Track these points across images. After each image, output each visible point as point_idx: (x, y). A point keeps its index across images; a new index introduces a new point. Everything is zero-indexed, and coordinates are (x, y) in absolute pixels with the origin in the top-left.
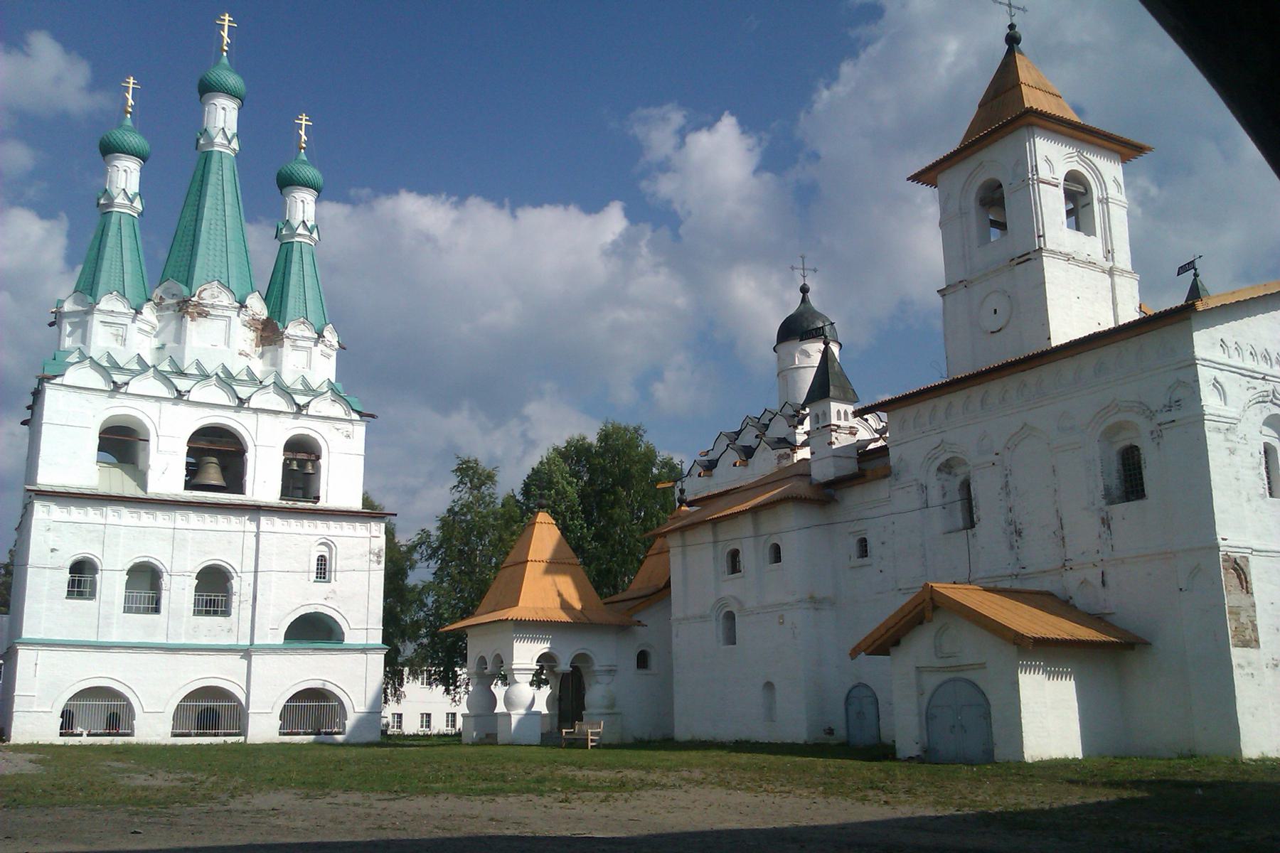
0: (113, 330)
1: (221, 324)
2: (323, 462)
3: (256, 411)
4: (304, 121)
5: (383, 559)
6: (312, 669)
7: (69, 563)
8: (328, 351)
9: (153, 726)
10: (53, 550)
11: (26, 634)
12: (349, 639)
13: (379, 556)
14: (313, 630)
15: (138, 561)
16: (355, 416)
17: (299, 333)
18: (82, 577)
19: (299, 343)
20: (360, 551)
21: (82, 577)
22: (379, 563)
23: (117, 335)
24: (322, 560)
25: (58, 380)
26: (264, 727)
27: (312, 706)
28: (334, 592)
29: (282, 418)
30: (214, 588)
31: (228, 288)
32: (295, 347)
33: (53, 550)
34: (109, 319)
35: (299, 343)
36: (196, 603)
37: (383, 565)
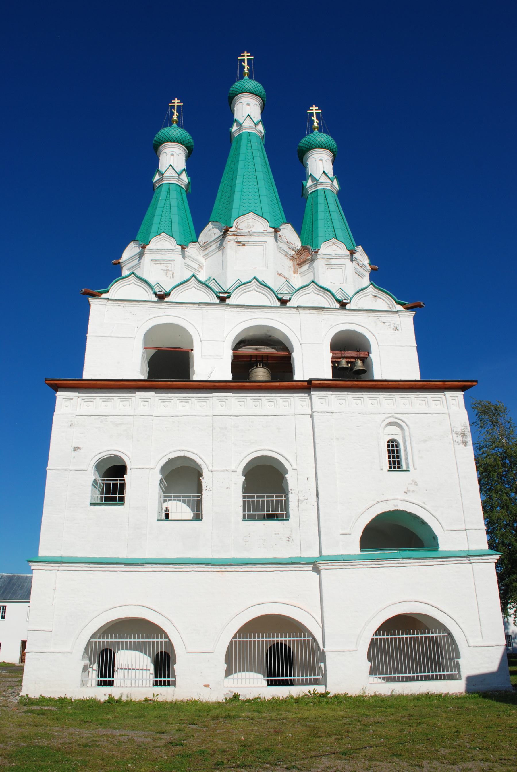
0: (163, 267)
1: (259, 249)
2: (373, 356)
3: (298, 308)
4: (314, 110)
5: (469, 439)
6: (404, 585)
7: (94, 462)
8: (361, 270)
9: (205, 677)
10: (76, 449)
11: (43, 552)
12: (444, 546)
13: (464, 435)
14: (396, 534)
15: (172, 456)
16: (399, 308)
17: (333, 253)
18: (112, 481)
19: (333, 261)
20: (441, 433)
21: (112, 481)
22: (465, 443)
23: (167, 271)
24: (393, 447)
25: (103, 296)
26: (348, 671)
27: (410, 640)
28: (416, 484)
29: (325, 315)
30: (266, 486)
31: (262, 217)
32: (329, 266)
33: (76, 449)
34: (159, 257)
35: (333, 261)
36: (246, 506)
37: (470, 447)
